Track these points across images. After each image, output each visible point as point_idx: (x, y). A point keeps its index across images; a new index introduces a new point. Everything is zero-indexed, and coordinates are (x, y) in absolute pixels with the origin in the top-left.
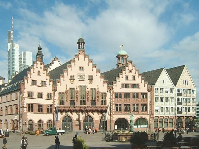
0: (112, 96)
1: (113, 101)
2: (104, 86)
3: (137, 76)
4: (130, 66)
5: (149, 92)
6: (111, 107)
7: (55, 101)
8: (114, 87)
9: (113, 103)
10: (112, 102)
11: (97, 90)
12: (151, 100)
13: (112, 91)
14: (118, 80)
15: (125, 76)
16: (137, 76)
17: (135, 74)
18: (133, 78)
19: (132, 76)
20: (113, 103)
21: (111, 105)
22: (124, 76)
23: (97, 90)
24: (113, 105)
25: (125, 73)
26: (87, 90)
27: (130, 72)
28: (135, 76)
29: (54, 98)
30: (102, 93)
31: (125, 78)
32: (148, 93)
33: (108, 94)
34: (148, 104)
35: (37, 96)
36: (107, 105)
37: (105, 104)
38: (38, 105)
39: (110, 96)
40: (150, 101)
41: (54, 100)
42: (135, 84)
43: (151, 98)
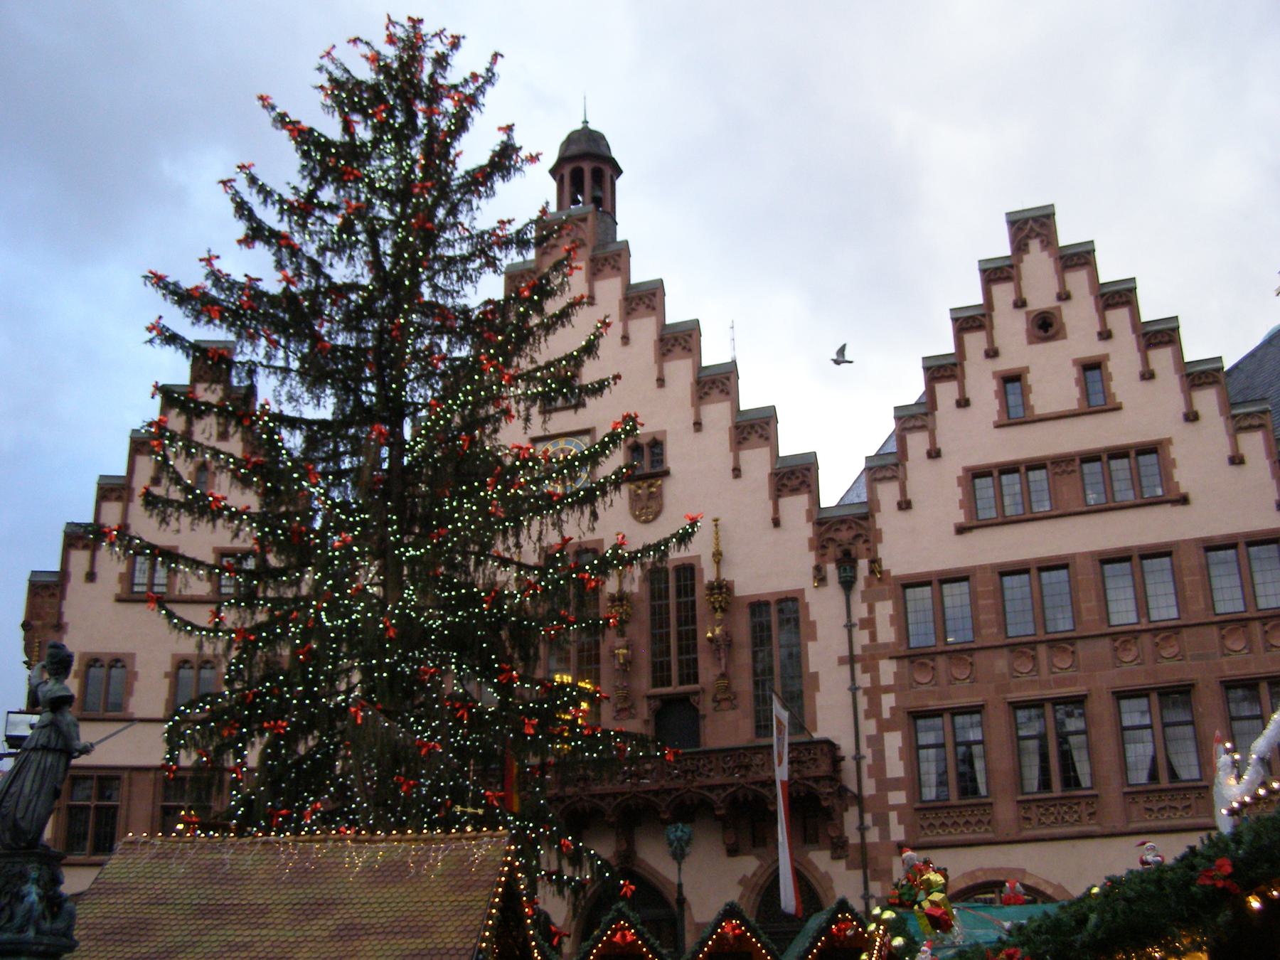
0: (869, 623)
2: (776, 523)
3: (1123, 358)
4: (1038, 264)
6: (866, 751)
8: (888, 519)
9: (888, 701)
10: (875, 692)
11: (709, 575)
13: (863, 564)
14: (917, 443)
15: (993, 385)
16: (1123, 358)
17: (1105, 335)
18: (1086, 393)
19: (1073, 373)
20: (888, 701)
21: (869, 727)
22: (981, 380)
23: (709, 575)
24: (884, 726)
25: (992, 353)
27: (1045, 327)
28: (1111, 366)
30: (758, 606)
31: (995, 405)
33: (825, 607)
35: (164, 687)
38: (166, 782)
39: (850, 627)
42: (1118, 453)
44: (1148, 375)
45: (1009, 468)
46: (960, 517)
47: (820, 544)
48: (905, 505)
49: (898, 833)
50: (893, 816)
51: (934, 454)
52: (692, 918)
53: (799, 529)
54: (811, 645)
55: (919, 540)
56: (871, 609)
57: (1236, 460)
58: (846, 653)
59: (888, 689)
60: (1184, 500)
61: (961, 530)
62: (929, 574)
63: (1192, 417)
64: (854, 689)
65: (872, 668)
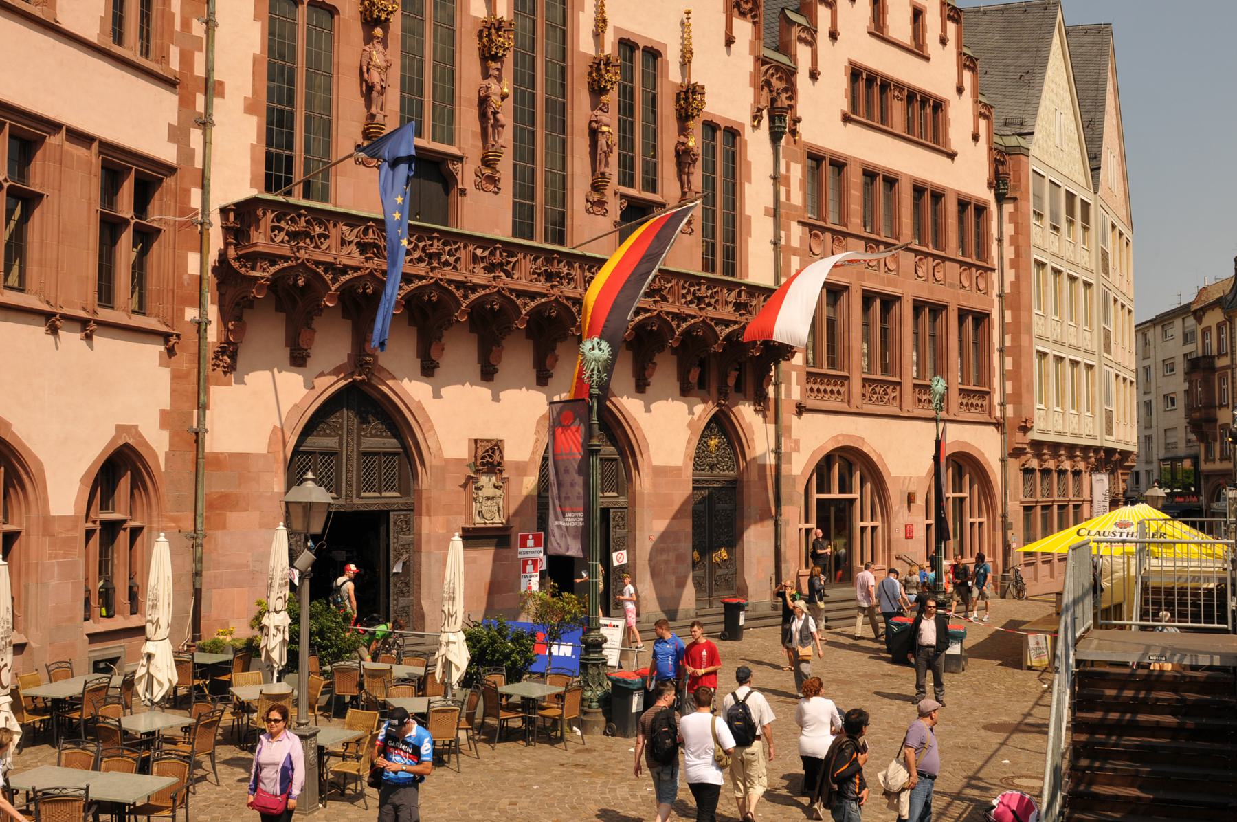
1: (795, 243)
5: (1000, 199)
7: (205, 124)
12: (1016, 285)
19: (909, 14)
23: (674, 75)
26: (585, 44)
29: (187, 60)
30: (711, 127)
32: (993, 207)
34: (995, 315)
36: (746, 281)
37: (731, 261)
40: (1007, 290)
41: (186, 103)
42: (925, 98)
43: (1014, 264)
44: (944, 41)
45: (872, 77)
46: (844, 105)
47: (762, 85)
48: (814, 75)
49: (796, 393)
50: (794, 374)
51: (833, 35)
52: (650, 462)
53: (743, 60)
54: (747, 185)
55: (821, 113)
56: (788, 169)
57: (975, 138)
58: (771, 205)
59: (795, 252)
60: (952, 156)
61: (846, 119)
62: (825, 150)
63: (960, 90)
64: (776, 244)
65: (788, 230)
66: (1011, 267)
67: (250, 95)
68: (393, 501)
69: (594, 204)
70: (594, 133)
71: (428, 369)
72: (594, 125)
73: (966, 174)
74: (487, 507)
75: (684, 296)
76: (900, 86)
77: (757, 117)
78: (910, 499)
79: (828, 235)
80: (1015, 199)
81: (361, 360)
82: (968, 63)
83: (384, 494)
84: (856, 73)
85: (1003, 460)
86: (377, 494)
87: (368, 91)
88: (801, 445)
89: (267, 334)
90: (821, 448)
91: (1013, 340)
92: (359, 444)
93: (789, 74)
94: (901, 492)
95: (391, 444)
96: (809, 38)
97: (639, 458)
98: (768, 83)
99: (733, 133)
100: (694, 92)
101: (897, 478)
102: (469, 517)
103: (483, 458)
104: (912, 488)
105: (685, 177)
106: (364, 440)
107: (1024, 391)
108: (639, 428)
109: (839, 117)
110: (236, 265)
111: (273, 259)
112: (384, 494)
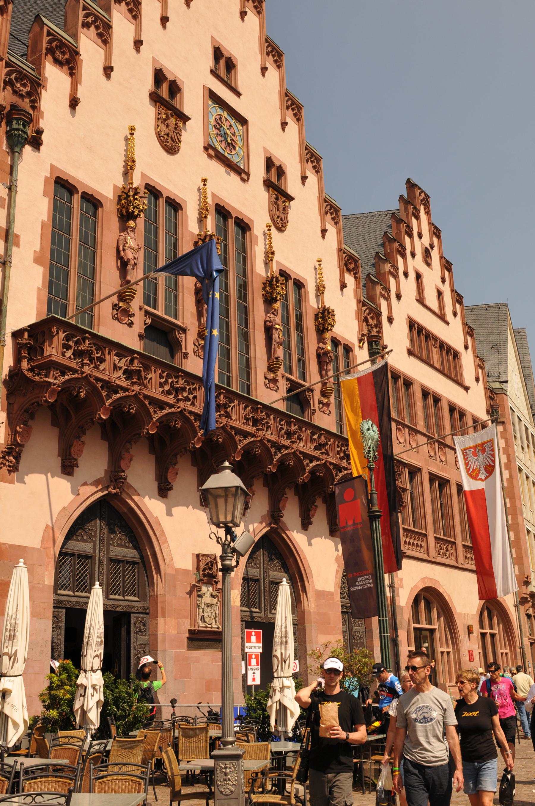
30: (335, 342)
44: (455, 314)
52: (314, 587)
66: (506, 469)
67: (38, 250)
68: (134, 604)
69: (270, 381)
70: (269, 330)
71: (164, 490)
72: (268, 324)
73: (475, 403)
74: (208, 613)
75: (339, 454)
76: (436, 338)
77: (360, 341)
78: (470, 631)
79: (407, 430)
80: (503, 423)
81: (115, 476)
82: (469, 331)
83: (127, 598)
84: (412, 324)
85: (516, 606)
86: (121, 597)
87: (124, 265)
88: (404, 583)
89: (44, 444)
90: (416, 586)
91: (512, 519)
92: (108, 551)
93: (378, 315)
94: (464, 625)
95: (132, 554)
96: (386, 295)
97: (306, 582)
98: (366, 320)
99: (348, 349)
100: (329, 313)
101: (460, 614)
102: (193, 621)
103: (204, 570)
104: (470, 623)
105: (324, 373)
106: (112, 548)
107: (524, 555)
108: (305, 558)
109: (406, 351)
110: (30, 375)
111: (64, 369)
112: (127, 598)
